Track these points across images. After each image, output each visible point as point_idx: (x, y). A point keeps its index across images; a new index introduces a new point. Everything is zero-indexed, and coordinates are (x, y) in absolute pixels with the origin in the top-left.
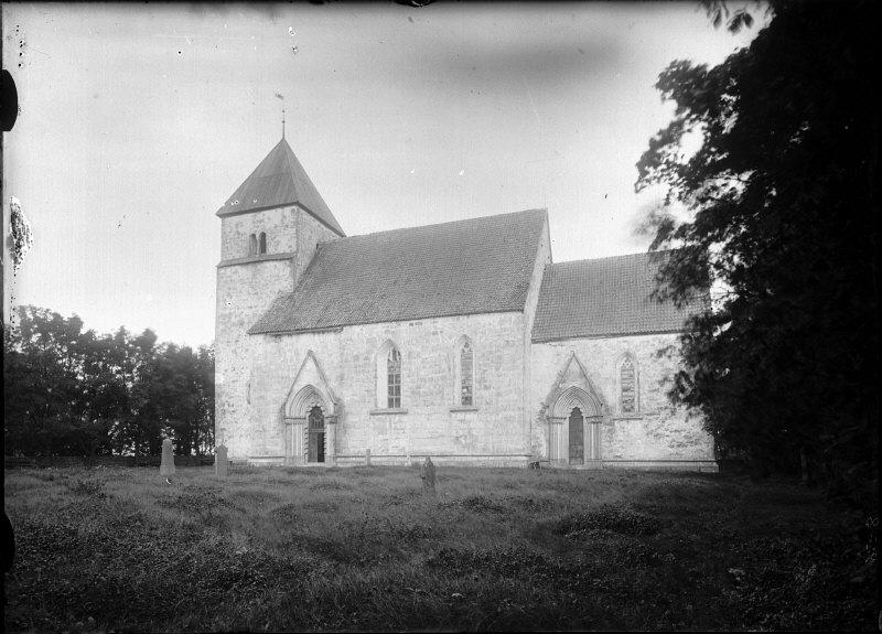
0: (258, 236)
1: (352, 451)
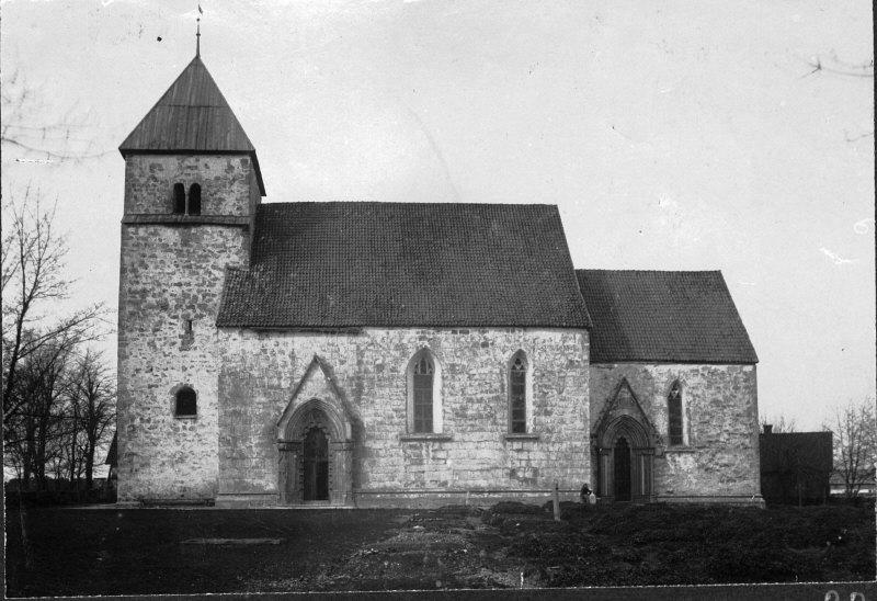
0: (187, 188)
1: (374, 485)
